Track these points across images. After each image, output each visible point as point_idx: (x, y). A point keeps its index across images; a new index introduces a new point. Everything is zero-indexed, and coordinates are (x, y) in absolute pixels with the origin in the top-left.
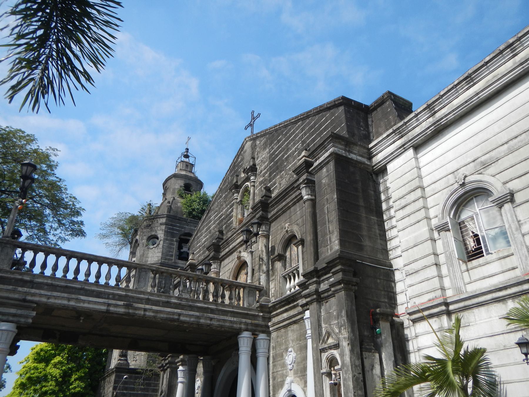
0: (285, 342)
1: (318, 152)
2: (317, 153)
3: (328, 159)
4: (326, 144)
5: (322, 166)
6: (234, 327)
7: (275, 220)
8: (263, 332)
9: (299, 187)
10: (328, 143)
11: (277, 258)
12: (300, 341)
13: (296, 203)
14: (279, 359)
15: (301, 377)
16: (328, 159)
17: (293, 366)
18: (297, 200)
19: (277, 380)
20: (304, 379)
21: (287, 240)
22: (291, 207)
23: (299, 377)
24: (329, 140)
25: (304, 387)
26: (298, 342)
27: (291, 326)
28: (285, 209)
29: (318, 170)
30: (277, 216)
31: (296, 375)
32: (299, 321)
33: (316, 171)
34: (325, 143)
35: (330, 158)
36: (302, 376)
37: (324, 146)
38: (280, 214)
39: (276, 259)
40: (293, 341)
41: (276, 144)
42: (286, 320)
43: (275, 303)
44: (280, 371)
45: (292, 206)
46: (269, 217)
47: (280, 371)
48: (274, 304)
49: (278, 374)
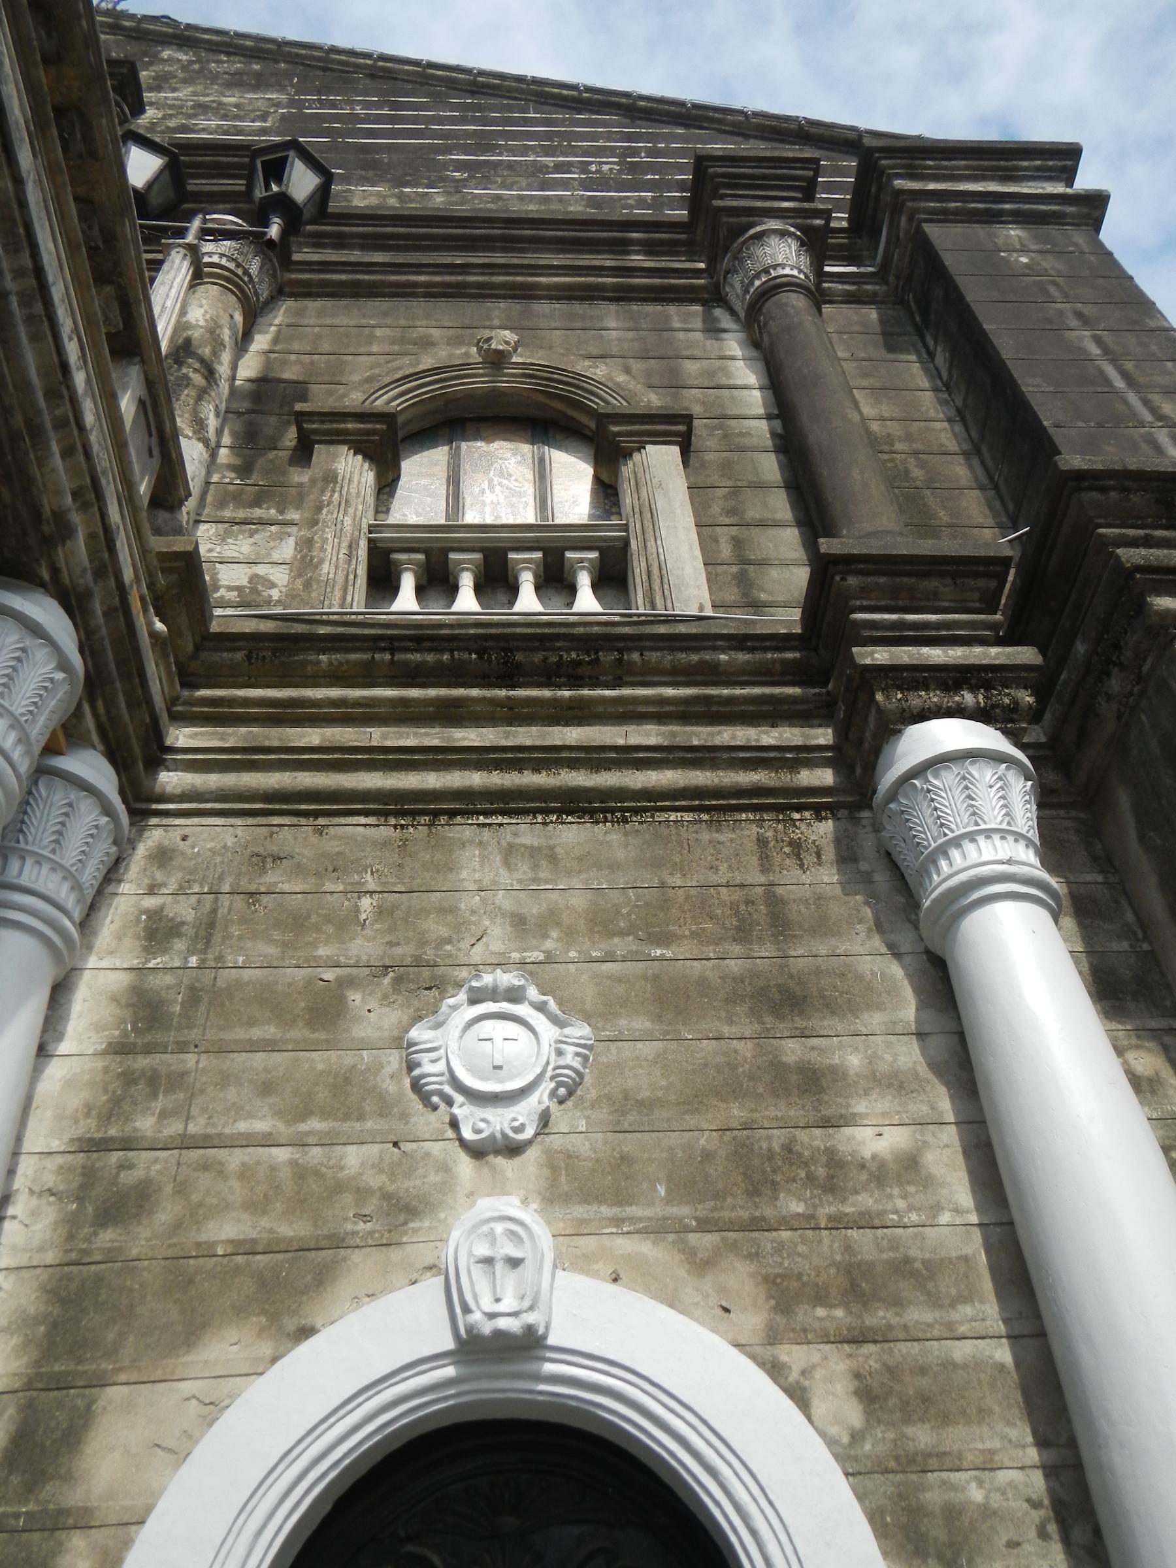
0: (381, 912)
1: (959, 168)
2: (946, 168)
3: (1056, 208)
4: (1026, 169)
5: (1002, 212)
6: (42, 461)
7: (332, 295)
8: (117, 757)
9: (744, 220)
10: (1038, 169)
11: (373, 432)
12: (664, 939)
13: (592, 298)
14: (269, 1031)
15: (704, 1241)
16: (1056, 208)
17: (545, 1119)
18: (617, 288)
19: (177, 1226)
20: (753, 1256)
21: (448, 401)
22: (540, 298)
23: (656, 1230)
24: (1060, 164)
25: (773, 1337)
26: (620, 945)
27: (500, 819)
28: (480, 285)
29: (956, 212)
30: (383, 284)
31: (606, 1211)
32: (636, 811)
33: (945, 212)
34: (1026, 164)
35: (1071, 209)
36: (705, 1226)
37: (1006, 169)
38: (416, 285)
39: (345, 432)
40: (519, 922)
41: (366, 105)
42: (463, 765)
43: (323, 630)
44: (268, 1141)
45: (550, 298)
46: (296, 257)
47: (268, 1141)
48: (300, 628)
49: (219, 1170)
